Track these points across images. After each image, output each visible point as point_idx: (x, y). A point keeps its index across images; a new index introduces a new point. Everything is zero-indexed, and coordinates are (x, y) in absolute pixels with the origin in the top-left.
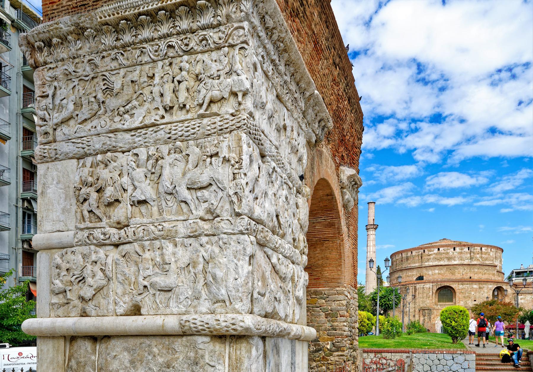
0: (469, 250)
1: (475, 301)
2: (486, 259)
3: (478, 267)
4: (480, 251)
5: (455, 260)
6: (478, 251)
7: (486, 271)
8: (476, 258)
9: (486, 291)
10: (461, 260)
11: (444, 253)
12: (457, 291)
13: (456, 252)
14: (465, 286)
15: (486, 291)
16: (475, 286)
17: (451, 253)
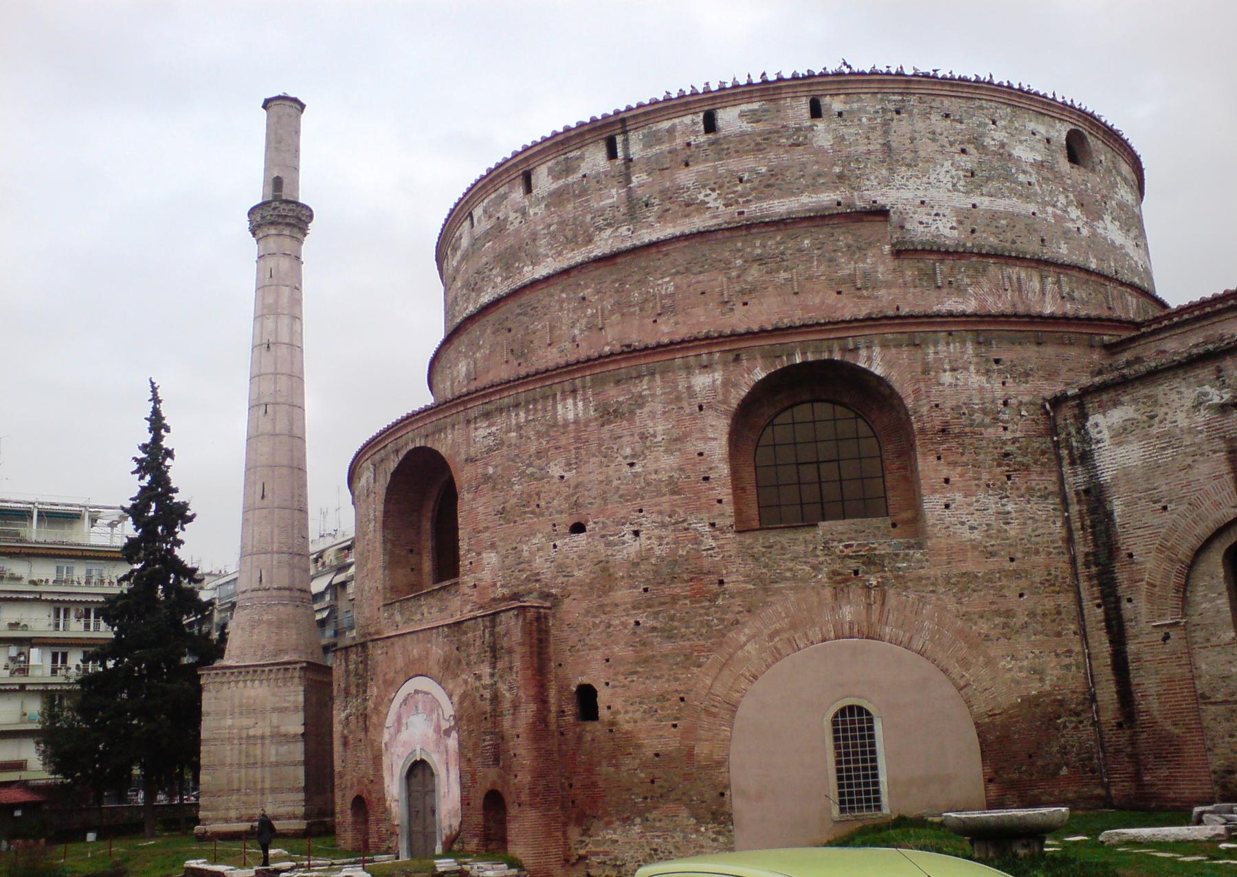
0: (612, 155)
1: (578, 528)
2: (772, 183)
3: (679, 256)
4: (703, 138)
5: (535, 260)
6: (679, 142)
7: (754, 273)
8: (668, 195)
9: (660, 428)
10: (572, 242)
11: (487, 235)
12: (463, 476)
13: (538, 201)
14: (500, 421)
15: (660, 428)
16: (569, 410)
17: (512, 216)
